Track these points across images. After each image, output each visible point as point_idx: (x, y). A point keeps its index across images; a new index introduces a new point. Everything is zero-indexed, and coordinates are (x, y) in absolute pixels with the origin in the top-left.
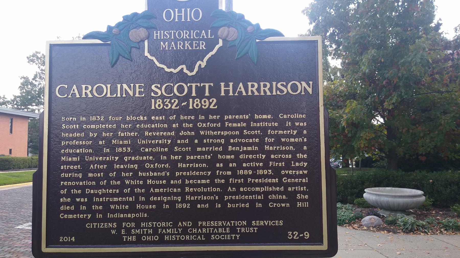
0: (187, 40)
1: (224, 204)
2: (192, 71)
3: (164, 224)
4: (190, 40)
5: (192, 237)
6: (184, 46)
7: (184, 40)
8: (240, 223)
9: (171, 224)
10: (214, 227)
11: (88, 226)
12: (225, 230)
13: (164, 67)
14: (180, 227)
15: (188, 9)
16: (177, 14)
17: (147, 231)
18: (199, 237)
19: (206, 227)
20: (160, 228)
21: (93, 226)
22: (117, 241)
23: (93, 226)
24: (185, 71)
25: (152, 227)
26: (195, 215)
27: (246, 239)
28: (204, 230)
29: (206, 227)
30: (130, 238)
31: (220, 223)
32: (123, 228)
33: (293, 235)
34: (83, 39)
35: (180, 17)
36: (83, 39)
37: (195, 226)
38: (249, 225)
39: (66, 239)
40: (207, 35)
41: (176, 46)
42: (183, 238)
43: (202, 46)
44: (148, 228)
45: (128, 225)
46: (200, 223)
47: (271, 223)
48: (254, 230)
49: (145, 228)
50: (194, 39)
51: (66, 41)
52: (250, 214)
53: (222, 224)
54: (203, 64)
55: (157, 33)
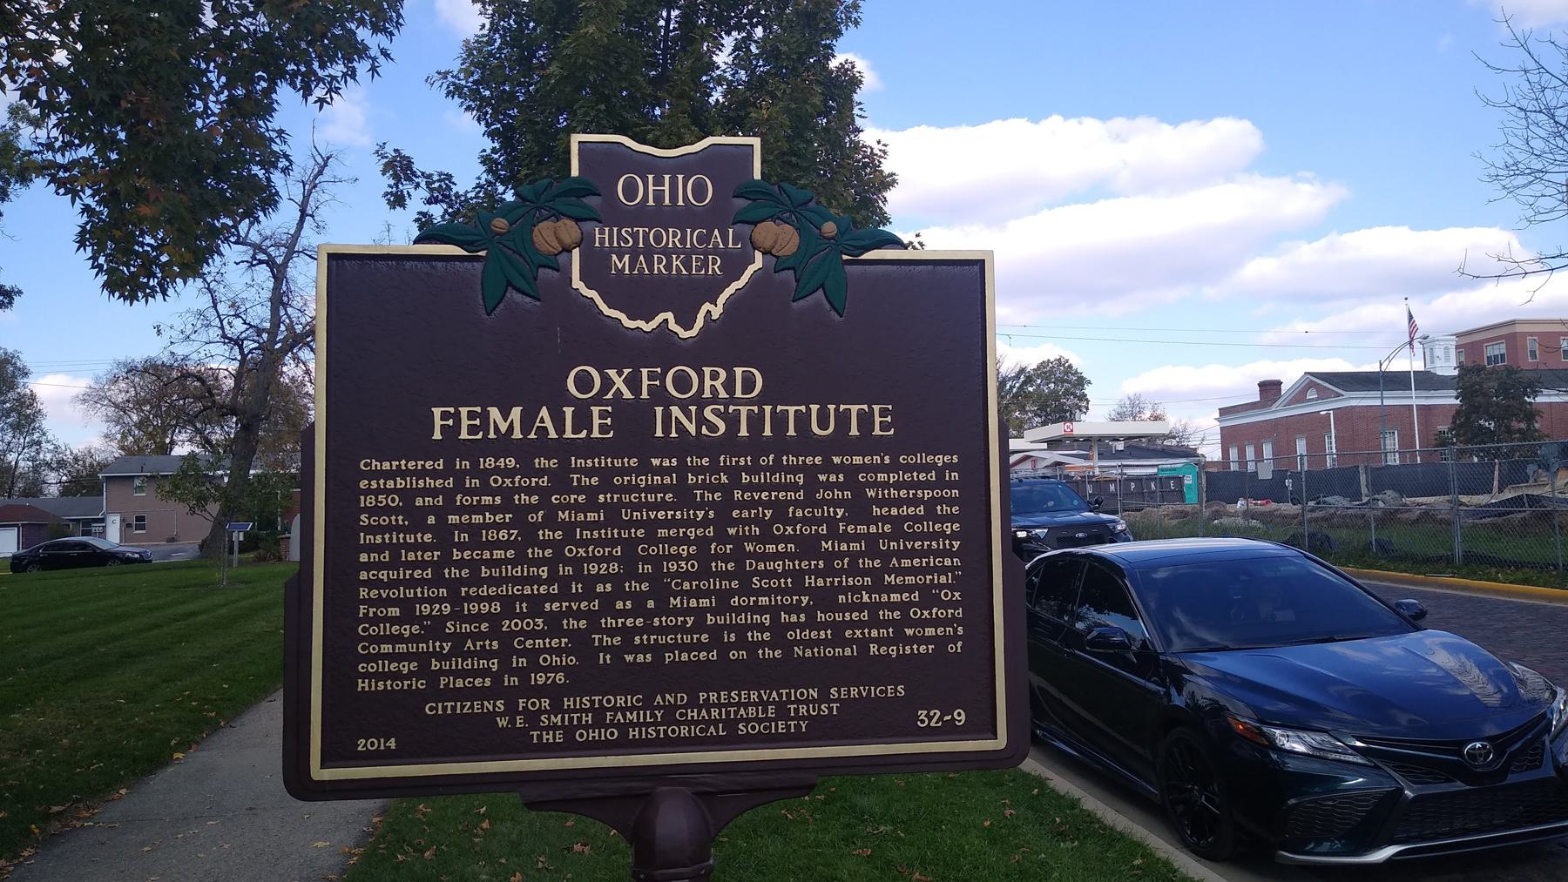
0: (675, 250)
1: (788, 647)
2: (688, 326)
3: (620, 701)
4: (684, 251)
5: (696, 731)
6: (669, 266)
7: (667, 252)
8: (802, 694)
9: (638, 700)
10: (739, 705)
11: (431, 709)
12: (765, 711)
13: (622, 317)
14: (659, 707)
15: (680, 177)
16: (651, 188)
17: (579, 719)
18: (712, 729)
19: (719, 706)
20: (609, 709)
21: (445, 708)
22: (519, 745)
23: (445, 708)
24: (673, 326)
25: (592, 709)
26: (695, 679)
27: (821, 731)
28: (715, 713)
29: (719, 706)
30: (548, 737)
31: (754, 696)
32: (520, 713)
33: (930, 718)
34: (415, 242)
35: (659, 196)
36: (415, 242)
37: (693, 703)
38: (824, 697)
39: (372, 744)
40: (725, 242)
41: (651, 267)
42: (675, 731)
43: (715, 267)
44: (581, 710)
45: (533, 704)
46: (702, 696)
47: (875, 692)
48: (830, 709)
49: (575, 711)
50: (694, 250)
51: (367, 247)
52: (824, 674)
53: (760, 696)
54: (717, 312)
55: (602, 232)
